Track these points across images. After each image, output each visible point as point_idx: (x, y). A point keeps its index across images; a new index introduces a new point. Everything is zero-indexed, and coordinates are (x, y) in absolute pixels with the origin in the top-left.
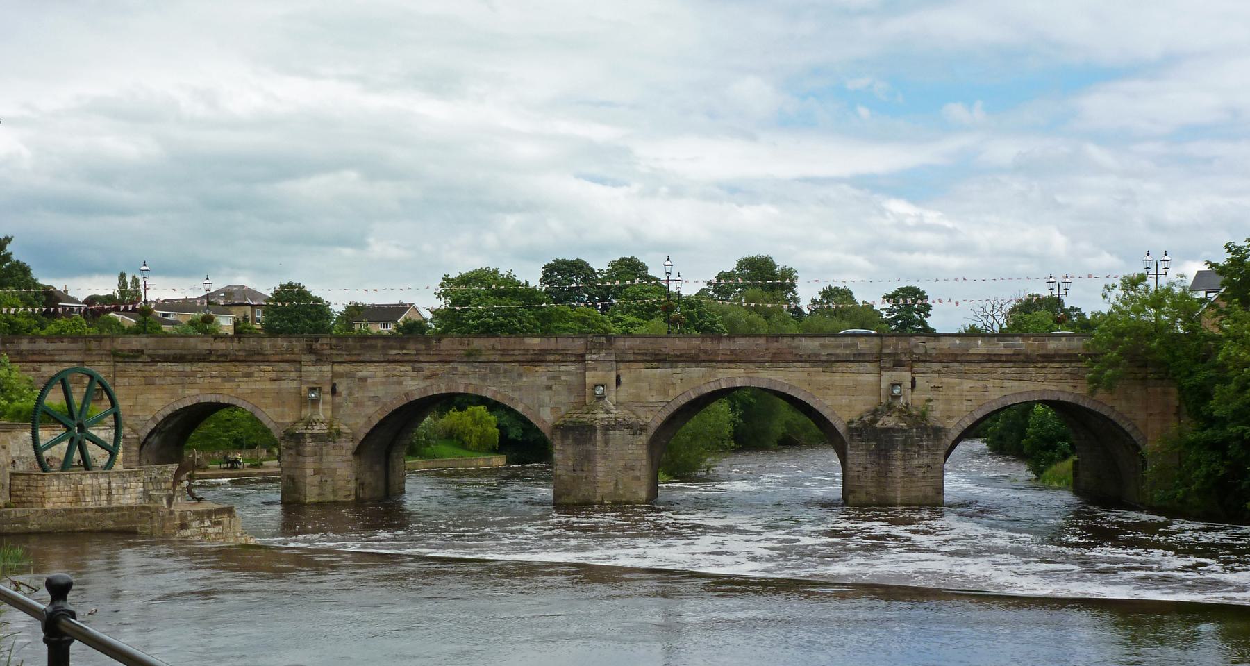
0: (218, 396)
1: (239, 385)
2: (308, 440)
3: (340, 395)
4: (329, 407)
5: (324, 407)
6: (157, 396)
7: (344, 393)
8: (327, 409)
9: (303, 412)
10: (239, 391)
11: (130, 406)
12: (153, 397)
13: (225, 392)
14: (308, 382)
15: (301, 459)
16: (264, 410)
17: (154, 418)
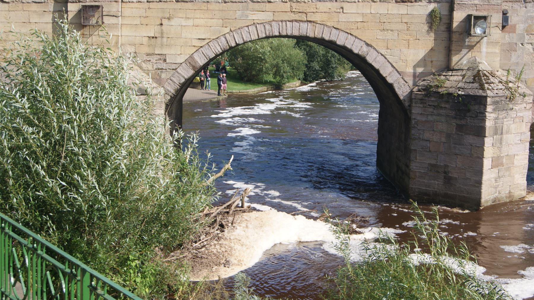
0: (304, 26)
1: (342, 8)
2: (489, 109)
3: (514, 31)
4: (497, 50)
5: (490, 50)
6: (198, 22)
7: (520, 28)
8: (495, 53)
9: (455, 59)
10: (342, 18)
11: (149, 37)
12: (190, 22)
13: (317, 18)
14: (463, 6)
15: (470, 139)
16: (383, 52)
17: (190, 61)
